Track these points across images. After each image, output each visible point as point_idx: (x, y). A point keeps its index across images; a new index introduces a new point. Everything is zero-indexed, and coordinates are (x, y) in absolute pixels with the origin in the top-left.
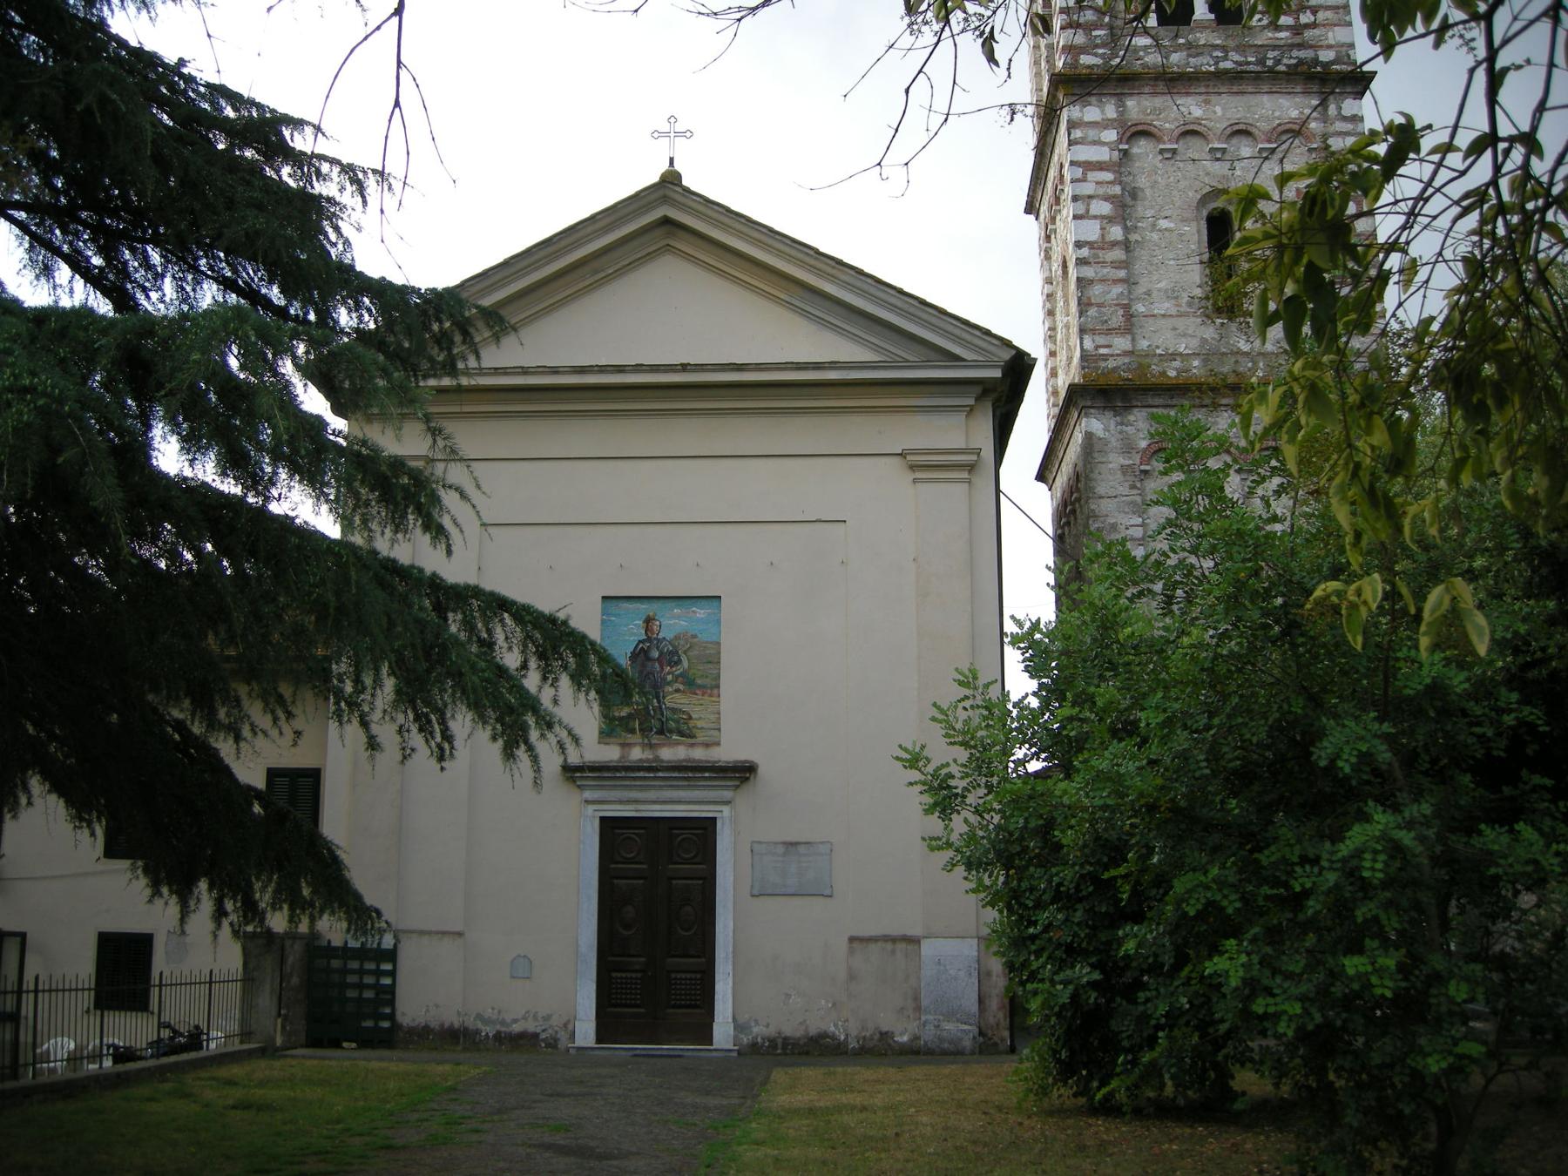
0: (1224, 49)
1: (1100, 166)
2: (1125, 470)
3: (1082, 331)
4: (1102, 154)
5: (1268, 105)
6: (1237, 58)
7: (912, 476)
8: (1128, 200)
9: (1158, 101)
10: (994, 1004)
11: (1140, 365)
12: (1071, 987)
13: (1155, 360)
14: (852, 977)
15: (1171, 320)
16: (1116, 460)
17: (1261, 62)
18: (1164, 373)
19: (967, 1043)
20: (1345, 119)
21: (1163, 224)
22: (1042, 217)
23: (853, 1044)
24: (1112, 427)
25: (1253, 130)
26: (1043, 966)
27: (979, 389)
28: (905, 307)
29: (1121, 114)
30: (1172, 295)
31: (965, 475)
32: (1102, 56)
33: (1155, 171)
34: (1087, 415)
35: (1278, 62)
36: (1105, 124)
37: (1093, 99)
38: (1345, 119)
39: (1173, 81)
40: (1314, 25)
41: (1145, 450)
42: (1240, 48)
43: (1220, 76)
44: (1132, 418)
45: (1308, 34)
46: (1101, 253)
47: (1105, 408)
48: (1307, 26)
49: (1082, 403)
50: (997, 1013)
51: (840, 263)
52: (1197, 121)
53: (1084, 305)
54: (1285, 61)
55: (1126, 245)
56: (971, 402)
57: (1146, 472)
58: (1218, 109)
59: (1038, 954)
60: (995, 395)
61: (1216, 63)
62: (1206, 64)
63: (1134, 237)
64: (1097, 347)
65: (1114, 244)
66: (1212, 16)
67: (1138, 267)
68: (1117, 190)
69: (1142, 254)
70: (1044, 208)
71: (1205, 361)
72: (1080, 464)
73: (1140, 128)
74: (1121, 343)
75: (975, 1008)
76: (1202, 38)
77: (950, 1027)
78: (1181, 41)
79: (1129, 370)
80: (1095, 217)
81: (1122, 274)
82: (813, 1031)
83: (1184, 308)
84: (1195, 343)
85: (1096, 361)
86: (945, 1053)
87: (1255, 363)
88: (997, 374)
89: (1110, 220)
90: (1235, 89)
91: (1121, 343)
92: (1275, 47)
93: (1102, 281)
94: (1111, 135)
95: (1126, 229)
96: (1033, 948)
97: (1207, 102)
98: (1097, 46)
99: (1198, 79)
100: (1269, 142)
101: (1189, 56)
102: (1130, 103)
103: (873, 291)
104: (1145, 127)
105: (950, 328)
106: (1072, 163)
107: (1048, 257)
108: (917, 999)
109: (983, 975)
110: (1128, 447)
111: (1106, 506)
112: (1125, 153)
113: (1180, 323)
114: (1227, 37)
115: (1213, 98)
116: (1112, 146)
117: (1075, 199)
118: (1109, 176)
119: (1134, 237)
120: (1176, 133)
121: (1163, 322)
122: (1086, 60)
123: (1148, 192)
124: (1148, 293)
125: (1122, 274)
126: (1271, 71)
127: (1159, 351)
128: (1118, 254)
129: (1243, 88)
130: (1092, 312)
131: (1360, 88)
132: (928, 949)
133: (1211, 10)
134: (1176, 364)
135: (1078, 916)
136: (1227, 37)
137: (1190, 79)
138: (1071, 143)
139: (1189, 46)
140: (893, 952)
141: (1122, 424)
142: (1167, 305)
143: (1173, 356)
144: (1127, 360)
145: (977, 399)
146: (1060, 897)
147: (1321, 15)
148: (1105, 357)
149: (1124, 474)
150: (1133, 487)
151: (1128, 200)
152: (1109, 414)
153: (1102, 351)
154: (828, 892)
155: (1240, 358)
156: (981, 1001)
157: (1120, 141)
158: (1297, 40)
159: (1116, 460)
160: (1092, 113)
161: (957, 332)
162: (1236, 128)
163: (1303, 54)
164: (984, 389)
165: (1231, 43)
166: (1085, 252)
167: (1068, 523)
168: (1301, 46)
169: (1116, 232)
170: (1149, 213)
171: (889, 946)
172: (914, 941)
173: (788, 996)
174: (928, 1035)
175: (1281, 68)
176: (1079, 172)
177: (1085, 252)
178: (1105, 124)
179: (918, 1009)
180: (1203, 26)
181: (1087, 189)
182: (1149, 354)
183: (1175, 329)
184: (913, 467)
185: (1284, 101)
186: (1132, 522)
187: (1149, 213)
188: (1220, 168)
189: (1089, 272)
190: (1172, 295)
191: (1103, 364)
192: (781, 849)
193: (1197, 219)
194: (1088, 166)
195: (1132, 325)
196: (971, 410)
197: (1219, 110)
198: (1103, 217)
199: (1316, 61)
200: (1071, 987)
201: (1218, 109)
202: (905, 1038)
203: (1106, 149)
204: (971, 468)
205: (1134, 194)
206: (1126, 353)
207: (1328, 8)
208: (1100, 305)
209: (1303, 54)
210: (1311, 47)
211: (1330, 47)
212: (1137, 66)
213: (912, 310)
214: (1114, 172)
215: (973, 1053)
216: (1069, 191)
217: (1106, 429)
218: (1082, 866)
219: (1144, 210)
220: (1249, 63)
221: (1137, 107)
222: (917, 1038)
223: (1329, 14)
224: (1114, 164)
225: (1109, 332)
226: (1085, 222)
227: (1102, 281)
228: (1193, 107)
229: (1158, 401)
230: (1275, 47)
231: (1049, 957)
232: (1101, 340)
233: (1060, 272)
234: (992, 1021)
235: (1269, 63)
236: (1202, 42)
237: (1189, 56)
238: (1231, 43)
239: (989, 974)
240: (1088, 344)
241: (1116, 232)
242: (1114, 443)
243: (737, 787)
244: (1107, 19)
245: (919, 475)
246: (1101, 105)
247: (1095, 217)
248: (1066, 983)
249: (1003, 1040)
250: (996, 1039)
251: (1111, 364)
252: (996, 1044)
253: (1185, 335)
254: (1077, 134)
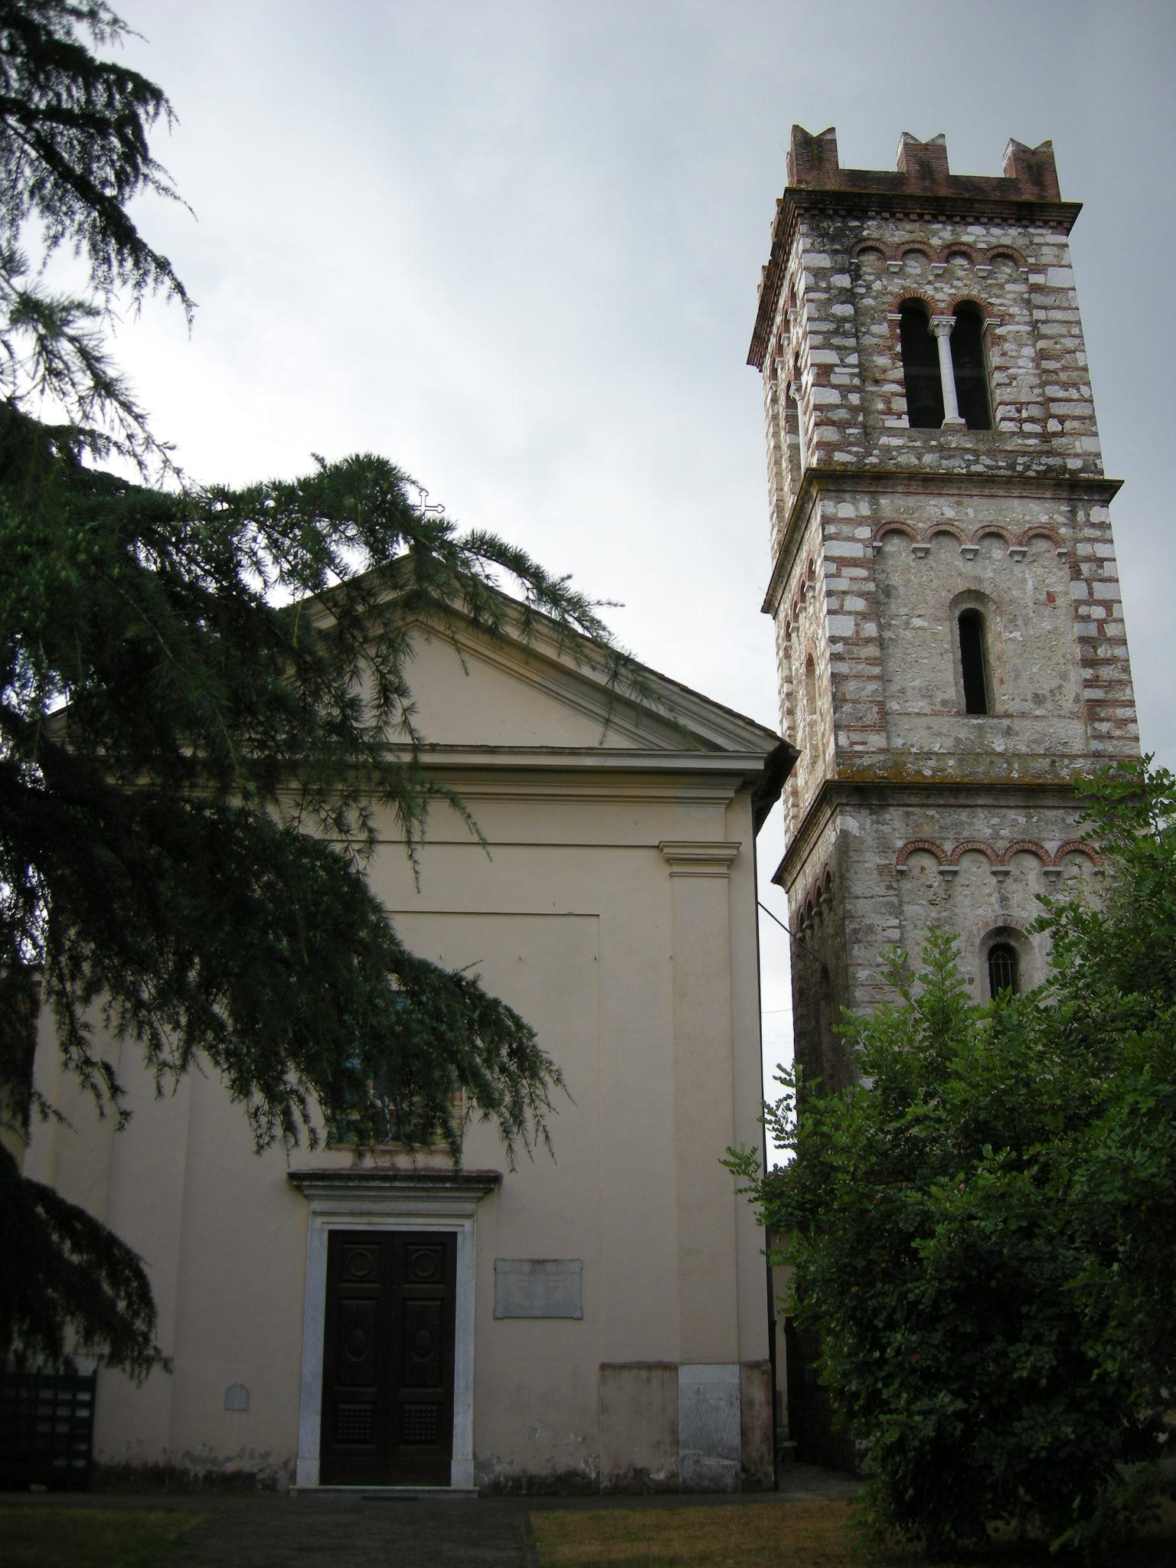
0: (975, 453)
1: (854, 562)
2: (881, 870)
3: (837, 727)
4: (856, 551)
5: (1019, 509)
6: (988, 462)
7: (668, 870)
8: (882, 597)
9: (911, 501)
10: (757, 1436)
11: (896, 764)
12: (934, 1418)
13: (911, 759)
14: (604, 1408)
15: (928, 720)
17: (1012, 467)
18: (919, 772)
19: (729, 1480)
20: (1093, 525)
21: (917, 622)
22: (781, 615)
23: (605, 1483)
24: (868, 826)
25: (1005, 533)
26: (898, 1396)
27: (738, 781)
29: (875, 511)
30: (926, 693)
32: (856, 454)
33: (908, 569)
34: (842, 813)
35: (1027, 468)
36: (859, 521)
37: (847, 496)
38: (1093, 525)
40: (1062, 434)
41: (901, 850)
42: (991, 453)
43: (972, 479)
44: (887, 817)
46: (855, 649)
47: (860, 806)
48: (1055, 434)
50: (759, 1445)
53: (838, 701)
54: (1035, 467)
55: (881, 642)
56: (731, 794)
57: (902, 872)
58: (970, 511)
59: (888, 1380)
61: (968, 467)
62: (957, 466)
63: (887, 634)
64: (852, 744)
65: (868, 640)
66: (963, 421)
67: (892, 665)
69: (896, 652)
70: (785, 608)
71: (961, 761)
72: (833, 863)
73: (894, 526)
74: (877, 741)
75: (737, 1441)
76: (954, 441)
77: (711, 1462)
78: (933, 443)
79: (885, 768)
80: (850, 613)
81: (876, 671)
82: (561, 1469)
84: (949, 743)
85: (850, 758)
86: (705, 1491)
87: (1010, 764)
88: (760, 765)
91: (877, 741)
92: (1024, 454)
93: (857, 677)
94: (865, 532)
95: (881, 627)
96: (882, 1374)
97: (959, 504)
98: (851, 444)
99: (950, 481)
100: (1021, 545)
101: (942, 458)
102: (884, 501)
104: (898, 526)
105: (712, 717)
107: (787, 656)
108: (674, 1432)
109: (746, 1405)
111: (861, 907)
112: (879, 550)
113: (936, 723)
115: (966, 500)
118: (862, 573)
119: (887, 634)
121: (917, 720)
122: (840, 457)
123: (902, 590)
124: (903, 691)
125: (876, 671)
126: (1021, 475)
127: (913, 750)
128: (872, 651)
129: (993, 491)
130: (847, 708)
132: (686, 1376)
133: (961, 415)
134: (932, 763)
135: (936, 1338)
137: (943, 480)
138: (825, 538)
139: (941, 448)
140: (649, 1380)
141: (878, 823)
143: (929, 755)
144: (882, 758)
145: (736, 792)
146: (920, 1319)
147: (1068, 425)
149: (880, 873)
150: (889, 887)
151: (882, 597)
152: (865, 812)
153: (858, 748)
154: (577, 1315)
155: (995, 759)
157: (874, 538)
158: (1045, 447)
160: (846, 510)
161: (719, 721)
162: (988, 530)
163: (1051, 461)
165: (982, 448)
166: (839, 647)
167: (811, 927)
168: (1049, 453)
169: (870, 629)
170: (903, 611)
171: (644, 1374)
172: (670, 1368)
173: (534, 1430)
174: (687, 1471)
177: (839, 647)
178: (859, 521)
179: (676, 1443)
180: (953, 429)
181: (842, 584)
182: (904, 752)
183: (929, 728)
184: (670, 861)
185: (1034, 506)
186: (889, 923)
187: (903, 611)
188: (968, 568)
189: (843, 668)
190: (926, 693)
191: (858, 761)
192: (527, 1268)
194: (843, 562)
195: (887, 722)
196: (730, 804)
197: (971, 513)
198: (857, 613)
199: (1064, 469)
200: (934, 1418)
201: (970, 511)
202: (662, 1476)
203: (860, 545)
204: (730, 862)
205: (888, 591)
206: (881, 751)
207: (1075, 418)
208: (855, 702)
209: (1051, 461)
210: (1059, 454)
211: (1077, 455)
212: (890, 465)
214: (869, 569)
215: (735, 1491)
216: (821, 585)
217: (862, 828)
218: (941, 1281)
219: (897, 608)
220: (1000, 468)
221: (890, 505)
222: (674, 1475)
223: (1076, 424)
224: (869, 561)
225: (864, 728)
226: (840, 617)
227: (857, 677)
228: (941, 508)
229: (914, 800)
230: (1024, 454)
231: (901, 1385)
232: (856, 737)
233: (803, 670)
235: (1020, 468)
236: (954, 445)
238: (982, 448)
240: (843, 740)
241: (870, 629)
243: (480, 1199)
244: (861, 418)
245: (676, 869)
247: (850, 613)
248: (926, 1414)
249: (767, 1475)
251: (866, 761)
252: (759, 1481)
253: (939, 734)
254: (831, 529)
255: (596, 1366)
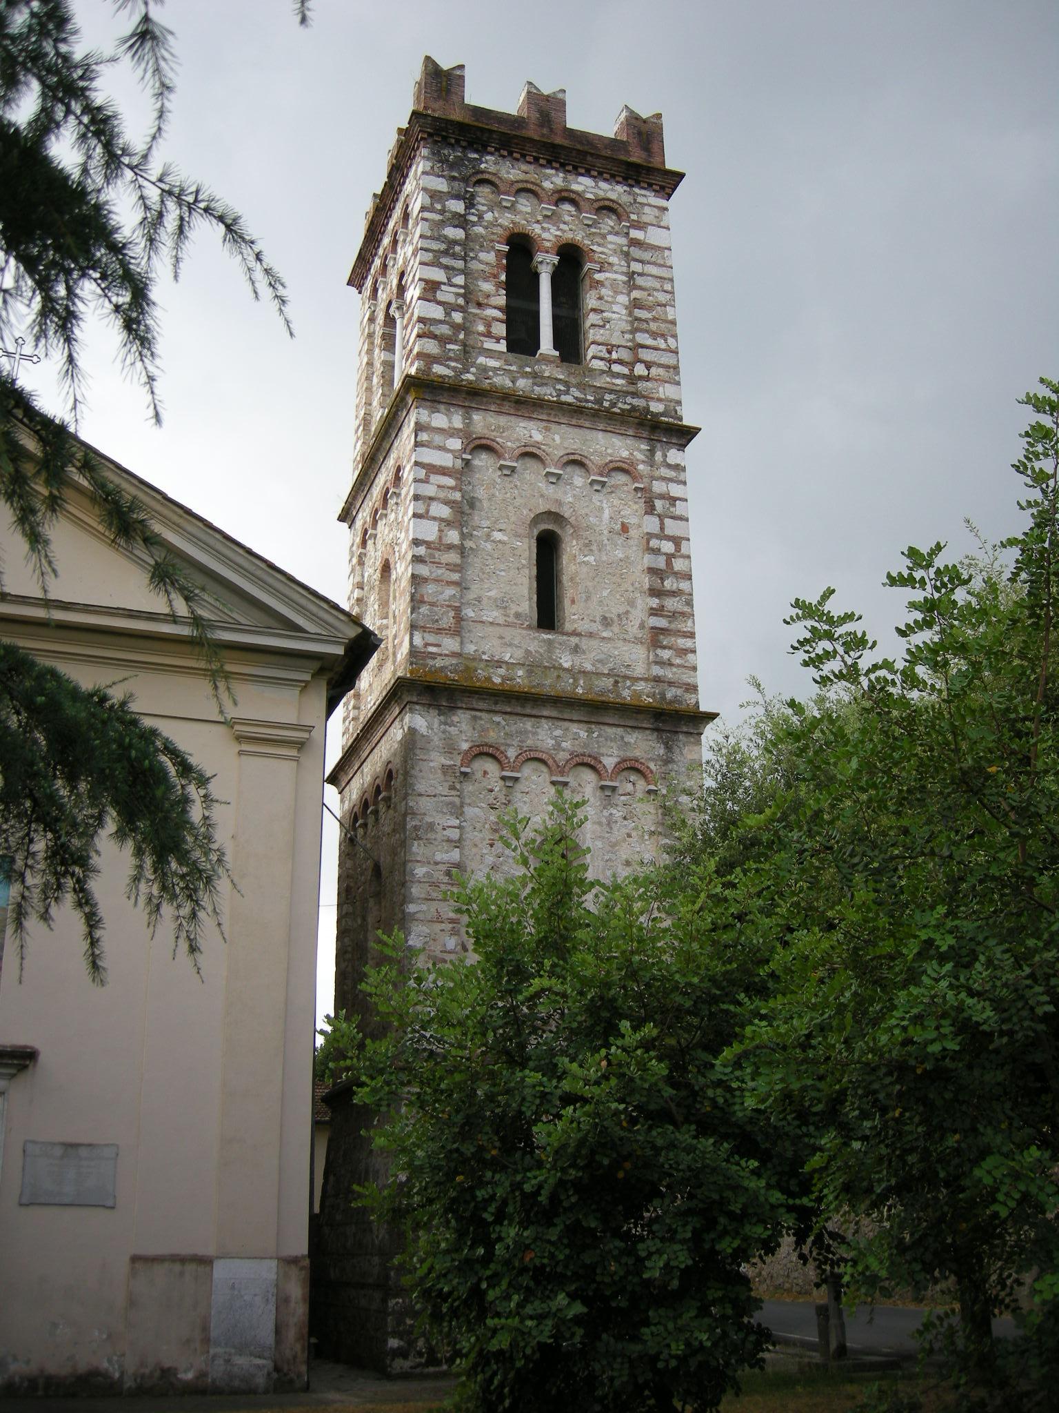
0: (567, 384)
1: (443, 471)
2: (445, 769)
3: (413, 627)
4: (446, 460)
5: (602, 442)
6: (578, 394)
7: (237, 747)
8: (466, 508)
9: (503, 420)
10: (291, 1334)
11: (467, 668)
12: (550, 1322)
13: (482, 665)
14: (132, 1302)
15: (498, 628)
16: (438, 759)
17: (599, 401)
18: (489, 679)
19: (260, 1380)
20: (669, 466)
21: (498, 536)
22: (359, 523)
23: (129, 1383)
24: (436, 725)
25: (587, 462)
26: (508, 1298)
27: (316, 665)
28: (252, 568)
29: (468, 425)
30: (501, 604)
31: (294, 753)
32: (454, 369)
33: (494, 484)
34: (411, 711)
35: (614, 405)
36: (451, 433)
37: (442, 407)
38: (669, 466)
39: (523, 405)
40: (647, 378)
41: (466, 752)
42: (582, 387)
43: (560, 407)
44: (456, 719)
45: (641, 385)
46: (437, 554)
47: (430, 705)
48: (641, 378)
49: (406, 698)
50: (294, 1345)
51: (189, 512)
52: (537, 445)
53: (416, 602)
54: (620, 405)
55: (462, 550)
56: (307, 677)
57: (465, 774)
58: (557, 437)
59: (494, 1280)
60: (329, 675)
61: (558, 396)
62: (548, 393)
63: (469, 544)
64: (426, 645)
65: (450, 547)
66: (557, 353)
67: (471, 573)
68: (457, 496)
69: (475, 562)
70: (363, 516)
71: (530, 672)
72: (397, 761)
73: (484, 442)
74: (450, 644)
75: (270, 1340)
76: (548, 370)
77: (242, 1361)
78: (528, 369)
79: (455, 671)
80: (434, 519)
81: (455, 577)
82: (82, 1368)
83: (511, 619)
84: (519, 654)
85: (424, 659)
86: (235, 1392)
87: (576, 680)
88: (339, 651)
89: (448, 523)
90: (574, 422)
91: (450, 644)
92: (611, 391)
93: (437, 581)
94: (455, 444)
95: (463, 536)
96: (488, 1273)
97: (547, 429)
98: (450, 359)
99: (541, 406)
100: (602, 475)
101: (534, 384)
102: (476, 417)
103: (219, 546)
104: (488, 442)
105: (296, 597)
106: (417, 464)
107: (361, 563)
108: (205, 1329)
109: (283, 1301)
110: (450, 748)
111: (424, 804)
112: (467, 463)
113: (509, 633)
114: (570, 374)
115: (553, 426)
116: (456, 454)
117: (416, 498)
118: (451, 482)
119: (469, 544)
120: (517, 452)
121: (491, 629)
122: (438, 369)
123: (486, 504)
124: (479, 599)
125: (455, 577)
126: (607, 410)
127: (485, 657)
128: (453, 557)
129: (581, 422)
130: (424, 609)
131: (683, 441)
132: (221, 1270)
133: (555, 348)
134: (502, 671)
135: (553, 1234)
136: (570, 374)
137: (534, 405)
138: (417, 444)
139: (534, 375)
140: (182, 1274)
141: (445, 724)
142: (495, 614)
143: (500, 663)
144: (454, 661)
145: (313, 676)
146: (539, 1212)
147: (654, 371)
148: (433, 656)
149: (444, 774)
150: (452, 788)
151: (466, 508)
152: (434, 712)
153: (431, 649)
154: (110, 1203)
155: (562, 674)
156: (278, 1331)
157: (464, 450)
158: (631, 388)
159: (438, 759)
160: (439, 420)
161: (303, 602)
162: (572, 457)
163: (636, 402)
164: (322, 665)
165: (573, 380)
166: (422, 550)
167: (365, 825)
168: (635, 394)
169: (453, 536)
170: (485, 523)
171: (177, 1267)
172: (205, 1262)
173: (55, 1325)
174: (217, 1371)
175: (616, 410)
176: (422, 473)
177: (422, 550)
178: (451, 433)
179: (206, 1341)
180: (546, 359)
181: (430, 490)
182: (476, 658)
183: (501, 638)
184: (239, 738)
185: (617, 441)
186: (450, 823)
187: (485, 523)
188: (550, 491)
189: (424, 570)
190: (501, 604)
191: (431, 662)
192: (58, 1151)
193: (529, 536)
194: (432, 469)
195: (462, 628)
196: (305, 687)
197: (561, 439)
198: (442, 520)
199: (647, 409)
200: (550, 1322)
201: (557, 437)
202: (190, 1376)
203: (450, 456)
204: (301, 745)
205: (472, 503)
206: (454, 655)
207: (660, 366)
208: (432, 604)
209: (636, 402)
210: (644, 397)
211: (660, 400)
212: (486, 384)
213: (259, 573)
214: (457, 479)
215: (266, 1392)
216: (408, 490)
217: (430, 727)
218: (563, 1170)
219: (480, 520)
220: (587, 401)
221: (483, 422)
222: (202, 1375)
223: (661, 371)
224: (457, 471)
225: (439, 631)
226: (424, 521)
227: (437, 581)
228: (529, 431)
229: (481, 705)
230: (611, 391)
231: (510, 1284)
232: (431, 638)
233: (378, 574)
234: (288, 1354)
235: (606, 404)
236: (547, 374)
237: (534, 384)
238: (573, 380)
239: (287, 1300)
240: (418, 640)
241: (453, 536)
242: (436, 741)
243: (13, 1076)
244: (462, 336)
245: (245, 747)
246: (448, 415)
247: (434, 519)
248: (540, 1318)
249: (299, 1375)
250: (292, 1375)
251: (439, 663)
252: (291, 1381)
253: (511, 645)
254: (424, 437)
255: (127, 1259)
